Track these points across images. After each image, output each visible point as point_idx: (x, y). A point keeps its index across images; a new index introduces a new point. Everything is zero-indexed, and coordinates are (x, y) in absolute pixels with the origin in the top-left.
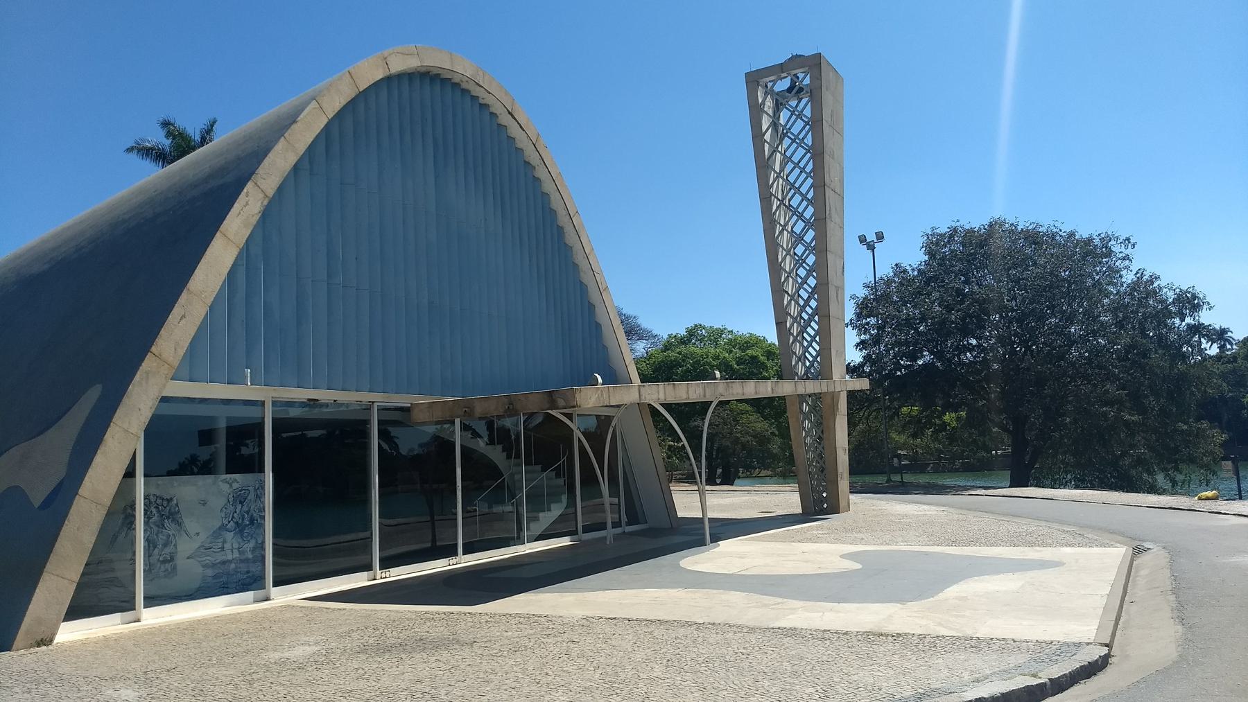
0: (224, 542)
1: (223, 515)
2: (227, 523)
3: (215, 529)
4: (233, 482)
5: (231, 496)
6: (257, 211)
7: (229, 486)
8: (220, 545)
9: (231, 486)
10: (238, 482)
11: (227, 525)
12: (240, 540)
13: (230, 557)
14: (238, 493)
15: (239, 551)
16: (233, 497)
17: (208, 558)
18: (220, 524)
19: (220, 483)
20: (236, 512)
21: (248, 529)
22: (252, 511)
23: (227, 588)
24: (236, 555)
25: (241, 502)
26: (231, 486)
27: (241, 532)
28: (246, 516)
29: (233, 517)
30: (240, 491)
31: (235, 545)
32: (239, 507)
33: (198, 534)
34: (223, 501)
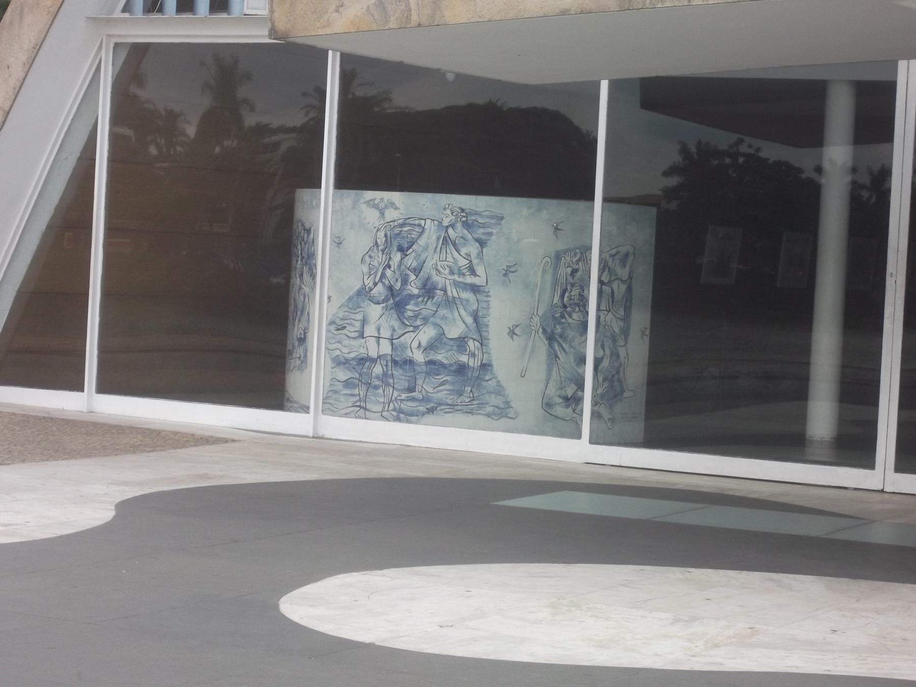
0: (364, 322)
1: (365, 269)
2: (371, 285)
3: (351, 293)
4: (386, 207)
5: (381, 234)
7: (377, 214)
8: (358, 325)
9: (382, 214)
10: (396, 208)
11: (371, 290)
12: (396, 324)
13: (373, 354)
14: (397, 230)
15: (392, 344)
16: (386, 236)
17: (339, 346)
18: (358, 286)
19: (364, 207)
20: (389, 267)
21: (417, 304)
22: (428, 269)
23: (365, 409)
24: (386, 348)
25: (401, 249)
26: (382, 214)
28: (413, 277)
29: (383, 275)
30: (403, 225)
31: (386, 333)
32: (397, 257)
34: (366, 242)
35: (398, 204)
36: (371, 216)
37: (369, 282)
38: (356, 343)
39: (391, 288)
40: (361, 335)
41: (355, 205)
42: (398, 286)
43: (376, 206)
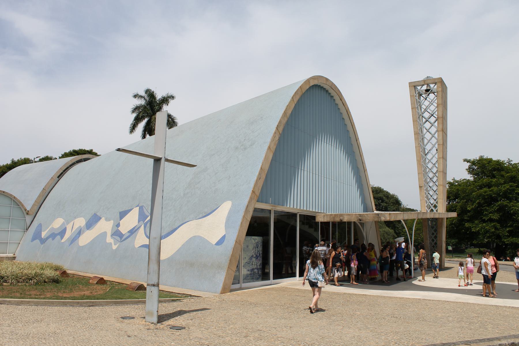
0: (253, 262)
6: (277, 139)
19: (252, 239)
27: (257, 258)
33: (245, 258)
35: (257, 239)
36: (253, 241)
37: (253, 254)
38: (252, 266)
39: (256, 255)
40: (252, 265)
41: (251, 239)
42: (257, 254)
43: (254, 239)
